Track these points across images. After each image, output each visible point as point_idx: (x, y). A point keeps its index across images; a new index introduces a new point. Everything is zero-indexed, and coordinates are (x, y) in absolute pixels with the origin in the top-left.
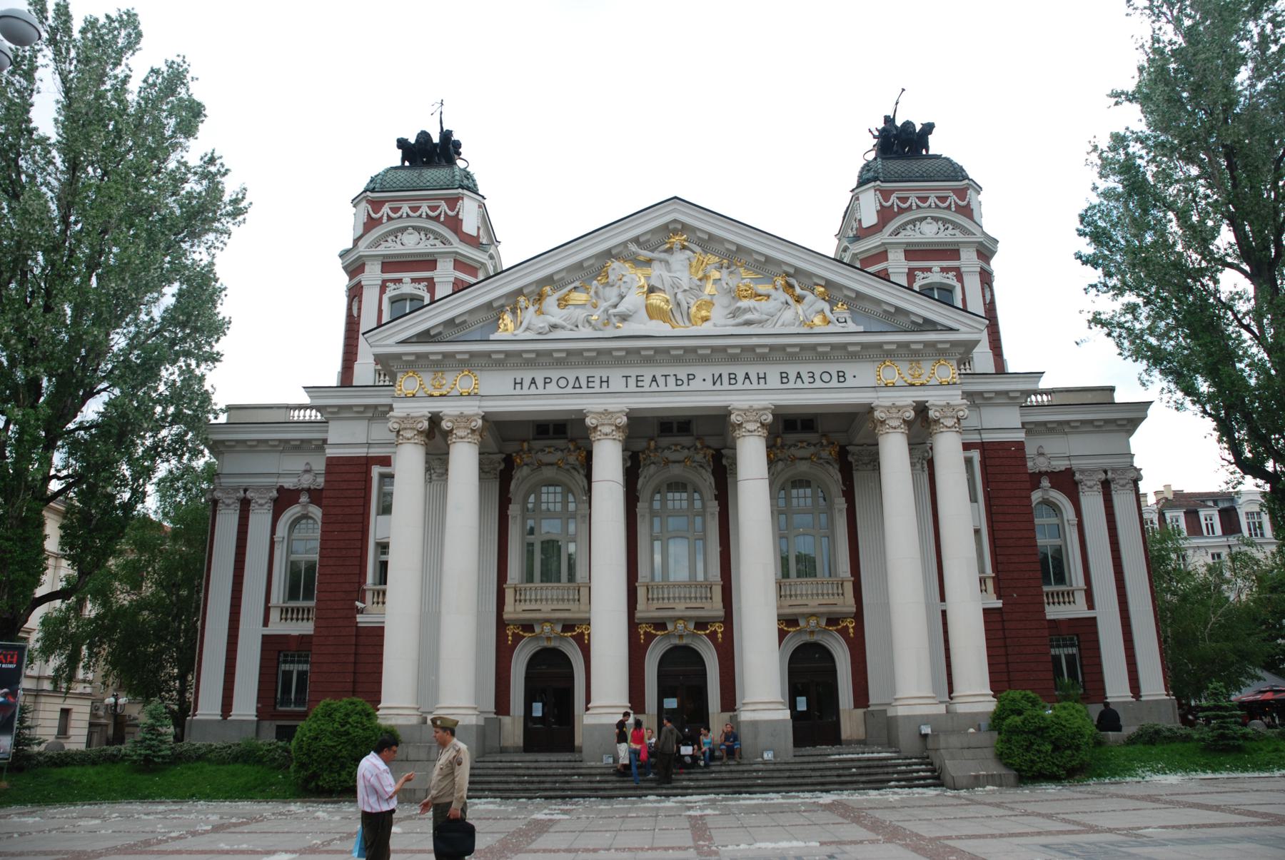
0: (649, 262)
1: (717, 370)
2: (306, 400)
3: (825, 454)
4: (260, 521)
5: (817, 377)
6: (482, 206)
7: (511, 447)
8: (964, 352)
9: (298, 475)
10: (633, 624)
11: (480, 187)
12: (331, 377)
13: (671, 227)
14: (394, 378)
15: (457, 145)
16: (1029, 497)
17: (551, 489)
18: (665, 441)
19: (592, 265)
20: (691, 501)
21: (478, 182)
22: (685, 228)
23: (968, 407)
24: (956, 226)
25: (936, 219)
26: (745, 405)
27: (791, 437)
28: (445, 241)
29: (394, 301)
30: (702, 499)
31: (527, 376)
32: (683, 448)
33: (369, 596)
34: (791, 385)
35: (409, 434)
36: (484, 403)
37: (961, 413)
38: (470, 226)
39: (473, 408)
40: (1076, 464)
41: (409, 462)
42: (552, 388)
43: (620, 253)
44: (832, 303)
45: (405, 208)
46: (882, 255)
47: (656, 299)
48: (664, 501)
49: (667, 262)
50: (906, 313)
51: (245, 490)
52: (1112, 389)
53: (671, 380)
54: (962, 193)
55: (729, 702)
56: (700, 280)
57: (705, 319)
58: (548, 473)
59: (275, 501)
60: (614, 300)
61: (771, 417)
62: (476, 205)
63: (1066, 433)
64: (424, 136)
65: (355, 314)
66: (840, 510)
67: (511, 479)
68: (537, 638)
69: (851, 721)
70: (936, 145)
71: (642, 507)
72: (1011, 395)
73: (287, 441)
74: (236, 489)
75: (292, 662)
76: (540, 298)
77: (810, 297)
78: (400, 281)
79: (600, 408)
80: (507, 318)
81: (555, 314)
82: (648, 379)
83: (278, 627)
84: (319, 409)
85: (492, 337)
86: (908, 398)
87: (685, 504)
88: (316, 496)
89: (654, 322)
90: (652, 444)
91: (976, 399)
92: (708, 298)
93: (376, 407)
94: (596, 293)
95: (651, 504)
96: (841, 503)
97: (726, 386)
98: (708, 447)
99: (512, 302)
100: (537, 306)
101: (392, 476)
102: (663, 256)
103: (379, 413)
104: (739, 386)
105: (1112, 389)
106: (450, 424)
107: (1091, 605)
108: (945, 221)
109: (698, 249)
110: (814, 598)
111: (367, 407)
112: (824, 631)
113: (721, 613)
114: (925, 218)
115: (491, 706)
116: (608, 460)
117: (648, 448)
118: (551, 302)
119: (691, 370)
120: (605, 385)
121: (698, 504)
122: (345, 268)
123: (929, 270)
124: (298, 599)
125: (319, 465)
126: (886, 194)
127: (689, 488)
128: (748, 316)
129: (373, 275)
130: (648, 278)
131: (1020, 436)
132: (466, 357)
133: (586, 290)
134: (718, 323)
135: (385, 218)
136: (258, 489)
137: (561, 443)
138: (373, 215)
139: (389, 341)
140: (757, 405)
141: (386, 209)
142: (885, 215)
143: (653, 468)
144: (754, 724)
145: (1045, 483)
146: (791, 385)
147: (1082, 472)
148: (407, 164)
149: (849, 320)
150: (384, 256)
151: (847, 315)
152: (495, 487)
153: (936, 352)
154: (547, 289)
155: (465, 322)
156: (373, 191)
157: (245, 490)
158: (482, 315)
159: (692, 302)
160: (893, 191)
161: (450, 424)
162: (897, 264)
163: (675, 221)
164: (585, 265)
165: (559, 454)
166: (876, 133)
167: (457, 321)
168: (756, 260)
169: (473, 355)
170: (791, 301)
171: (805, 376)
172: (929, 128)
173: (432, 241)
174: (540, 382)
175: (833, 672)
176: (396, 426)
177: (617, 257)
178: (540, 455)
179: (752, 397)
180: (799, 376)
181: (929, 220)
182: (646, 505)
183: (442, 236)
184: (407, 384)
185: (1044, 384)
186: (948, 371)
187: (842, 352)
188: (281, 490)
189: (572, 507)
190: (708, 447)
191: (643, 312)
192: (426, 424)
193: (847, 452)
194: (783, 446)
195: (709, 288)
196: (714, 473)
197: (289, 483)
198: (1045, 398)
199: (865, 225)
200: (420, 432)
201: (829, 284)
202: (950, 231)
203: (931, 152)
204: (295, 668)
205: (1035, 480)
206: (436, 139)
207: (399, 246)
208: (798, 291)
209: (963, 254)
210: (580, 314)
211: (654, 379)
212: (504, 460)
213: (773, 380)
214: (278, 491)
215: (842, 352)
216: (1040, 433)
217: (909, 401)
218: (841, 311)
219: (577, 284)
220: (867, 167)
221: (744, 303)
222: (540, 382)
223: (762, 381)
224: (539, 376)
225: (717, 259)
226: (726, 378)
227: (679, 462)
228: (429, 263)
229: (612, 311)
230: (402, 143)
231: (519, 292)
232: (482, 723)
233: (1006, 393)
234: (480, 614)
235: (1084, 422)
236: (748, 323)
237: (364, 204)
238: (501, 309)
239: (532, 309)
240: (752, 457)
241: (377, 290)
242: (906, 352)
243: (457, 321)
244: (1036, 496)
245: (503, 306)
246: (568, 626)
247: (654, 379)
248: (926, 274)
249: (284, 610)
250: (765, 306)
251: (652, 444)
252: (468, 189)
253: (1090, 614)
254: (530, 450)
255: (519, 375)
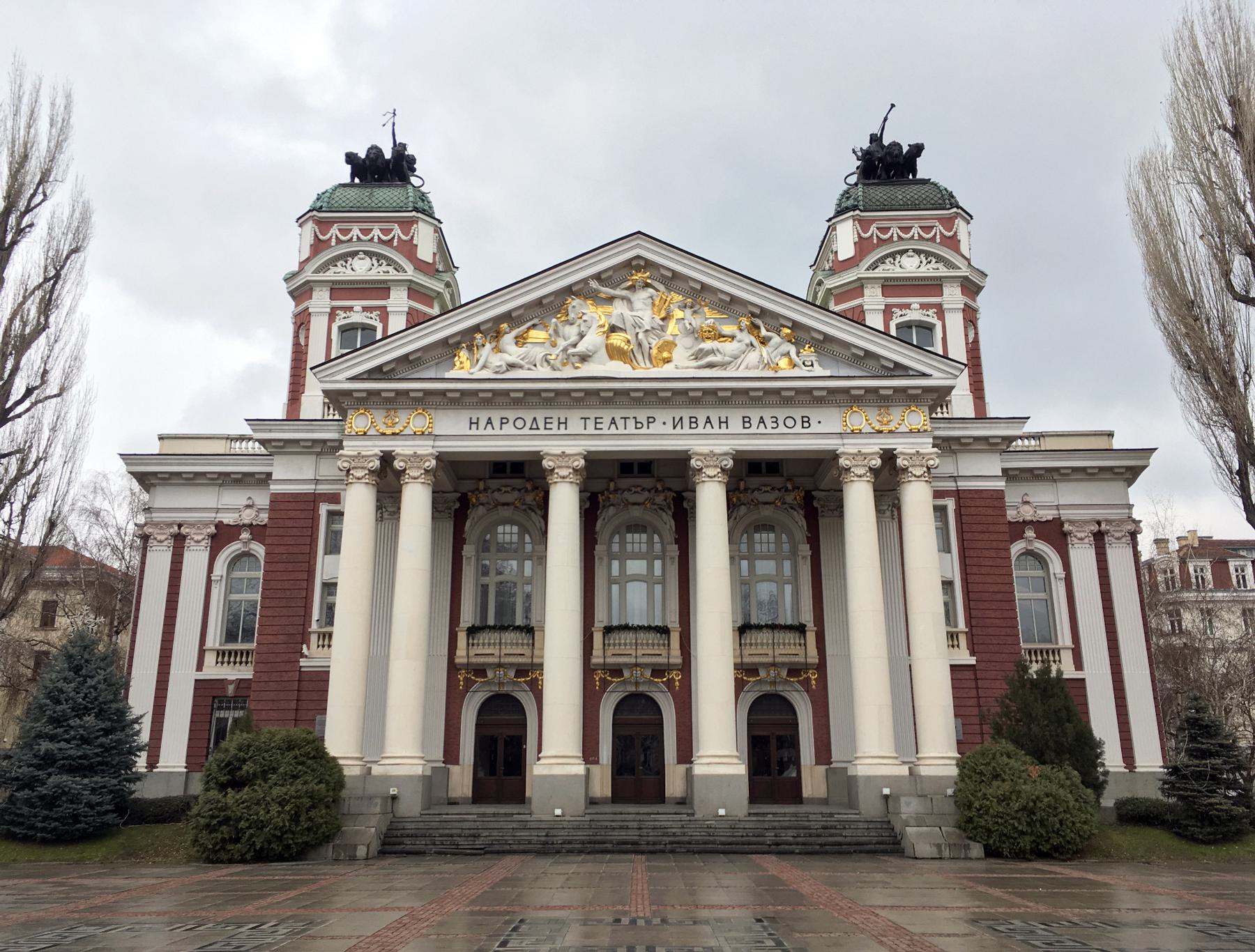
0: (610, 300)
1: (677, 414)
2: (247, 430)
3: (789, 499)
4: (195, 559)
5: (781, 422)
6: (439, 231)
7: (467, 486)
8: (939, 397)
9: (239, 510)
10: (588, 669)
11: (435, 209)
12: (275, 407)
13: (634, 263)
14: (344, 413)
15: (412, 160)
16: (1008, 550)
17: (508, 528)
18: (625, 482)
19: (552, 302)
20: (650, 543)
21: (433, 204)
22: (649, 265)
23: (939, 456)
24: (940, 259)
25: (918, 252)
26: (705, 450)
27: (755, 481)
28: (398, 268)
29: (344, 330)
30: (662, 542)
31: (483, 416)
32: (643, 489)
33: (314, 638)
34: (753, 430)
35: (359, 473)
36: (437, 443)
37: (931, 462)
38: (426, 251)
39: (426, 448)
40: (1065, 514)
41: (359, 502)
42: (509, 429)
43: (581, 290)
44: (798, 344)
45: (356, 232)
46: (858, 288)
47: (617, 340)
48: (623, 542)
49: (629, 301)
50: (877, 357)
51: (180, 526)
52: (1110, 435)
53: (631, 423)
54: (948, 222)
55: (686, 754)
56: (663, 319)
57: (668, 361)
58: (505, 512)
59: (213, 537)
60: (574, 338)
61: (731, 462)
62: (432, 229)
63: (1055, 481)
64: (375, 152)
65: (302, 342)
66: (804, 557)
67: (466, 518)
68: (489, 683)
69: (813, 781)
70: (924, 168)
71: (599, 549)
72: (991, 441)
73: (228, 474)
74: (170, 525)
75: (228, 708)
76: (498, 335)
77: (776, 339)
78: (350, 309)
79: (558, 451)
80: (463, 354)
81: (513, 352)
82: (607, 421)
83: (213, 671)
84: (263, 442)
85: (447, 375)
86: (874, 446)
87: (644, 547)
88: (258, 532)
89: (614, 362)
90: (612, 485)
91: (947, 446)
92: (671, 338)
93: (324, 441)
94: (556, 332)
95: (610, 547)
96: (805, 549)
97: (687, 430)
98: (669, 489)
99: (467, 339)
100: (494, 344)
101: (342, 514)
102: (625, 293)
103: (329, 449)
104: (700, 430)
105: (1110, 435)
106: (402, 464)
107: (1079, 665)
108: (928, 254)
109: (661, 288)
111: (315, 441)
112: (786, 682)
113: (679, 661)
114: (907, 251)
115: (439, 754)
116: (564, 504)
117: (608, 490)
118: (508, 340)
119: (650, 413)
120: (563, 426)
121: (658, 547)
122: (291, 293)
123: (908, 306)
124: (236, 641)
125: (262, 500)
126: (864, 224)
127: (649, 529)
128: (710, 359)
129: (320, 301)
130: (609, 315)
131: (1000, 484)
132: (421, 394)
133: (546, 327)
134: (681, 366)
135: (333, 242)
136: (192, 525)
137: (518, 482)
138: (321, 237)
139: (341, 379)
140: (718, 450)
141: (334, 231)
142: (863, 247)
143: (612, 510)
144: (707, 778)
145: (1030, 534)
146: (753, 430)
147: (1072, 522)
148: (357, 180)
149: (816, 364)
150: (334, 282)
151: (814, 359)
152: (449, 527)
153: (906, 398)
154: (504, 326)
155: (419, 358)
156: (320, 210)
157: (180, 526)
158: (439, 351)
159: (654, 343)
160: (873, 221)
161: (402, 464)
162: (873, 300)
163: (638, 257)
164: (544, 302)
165: (516, 494)
166: (860, 154)
167: (411, 358)
168: (721, 300)
169: (427, 393)
170: (756, 343)
171: (768, 421)
172: (917, 150)
173: (384, 268)
174: (496, 423)
175: (795, 725)
176: (346, 465)
177: (577, 294)
178: (496, 495)
179: (712, 442)
180: (762, 421)
181: (910, 253)
182: (605, 547)
183: (396, 262)
184: (358, 422)
185: (1029, 428)
186: (918, 418)
187: (808, 397)
188: (219, 525)
189: (528, 548)
190: (669, 489)
191: (603, 351)
192: (377, 463)
193: (813, 498)
194: (746, 490)
195: (672, 327)
196: (675, 517)
197: (228, 519)
198: (1033, 442)
199: (841, 258)
200: (371, 472)
201: (796, 325)
202: (933, 265)
203: (918, 177)
204: (230, 715)
206: (388, 155)
207: (349, 271)
208: (764, 332)
209: (946, 290)
210: (538, 352)
211: (613, 422)
212: (459, 499)
213: (736, 426)
214: (217, 526)
215: (808, 397)
216: (1027, 480)
217: (876, 449)
218: (808, 353)
219: (535, 321)
220: (846, 195)
221: (707, 345)
222: (496, 423)
223: (724, 425)
224: (496, 416)
225: (680, 298)
226: (686, 421)
227: (638, 504)
228: (381, 289)
229: (571, 350)
230: (351, 158)
231: (476, 328)
232: (428, 773)
233: (985, 439)
234: (430, 656)
235: (1075, 470)
236: (711, 366)
237: (310, 226)
238: (457, 346)
239: (488, 346)
240: (711, 502)
241: (326, 318)
242: (873, 398)
243: (411, 358)
244: (1017, 548)
245: (459, 343)
246: (522, 671)
247: (613, 422)
248: (904, 312)
249: (220, 653)
250: (729, 347)
251: (612, 485)
252: (423, 212)
253: (1078, 675)
254: (485, 490)
255: (475, 415)
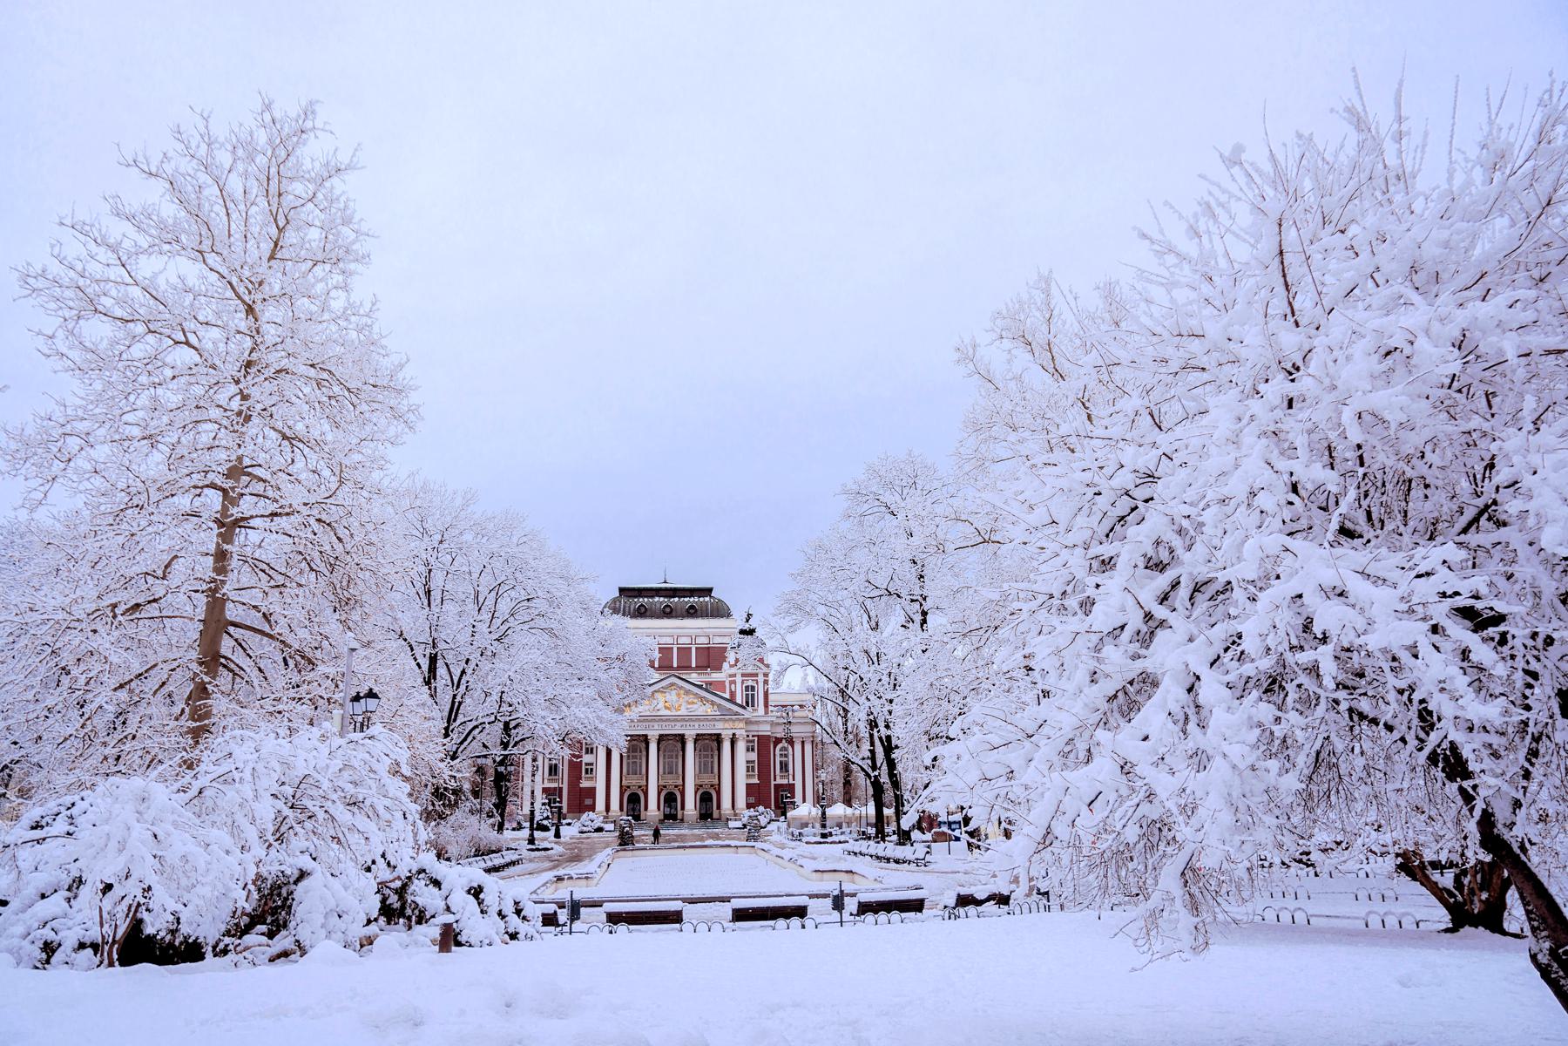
110: (707, 780)
116: (653, 747)
134: (683, 711)
179: (690, 733)
186: (742, 725)
205: (778, 741)
